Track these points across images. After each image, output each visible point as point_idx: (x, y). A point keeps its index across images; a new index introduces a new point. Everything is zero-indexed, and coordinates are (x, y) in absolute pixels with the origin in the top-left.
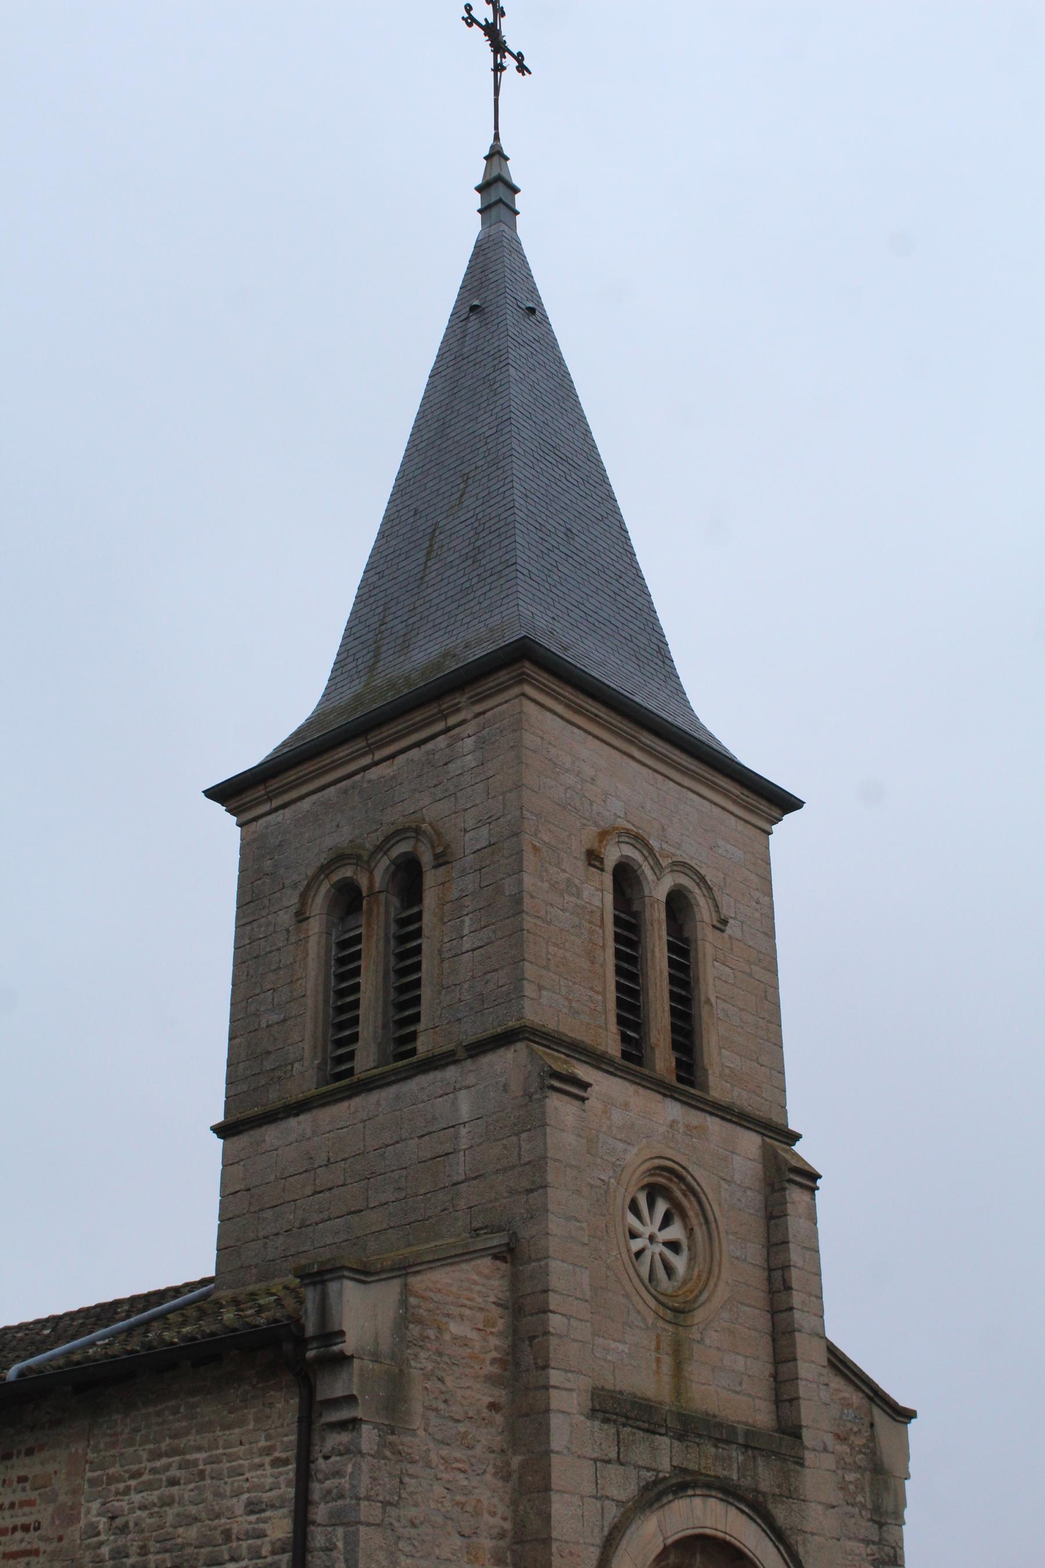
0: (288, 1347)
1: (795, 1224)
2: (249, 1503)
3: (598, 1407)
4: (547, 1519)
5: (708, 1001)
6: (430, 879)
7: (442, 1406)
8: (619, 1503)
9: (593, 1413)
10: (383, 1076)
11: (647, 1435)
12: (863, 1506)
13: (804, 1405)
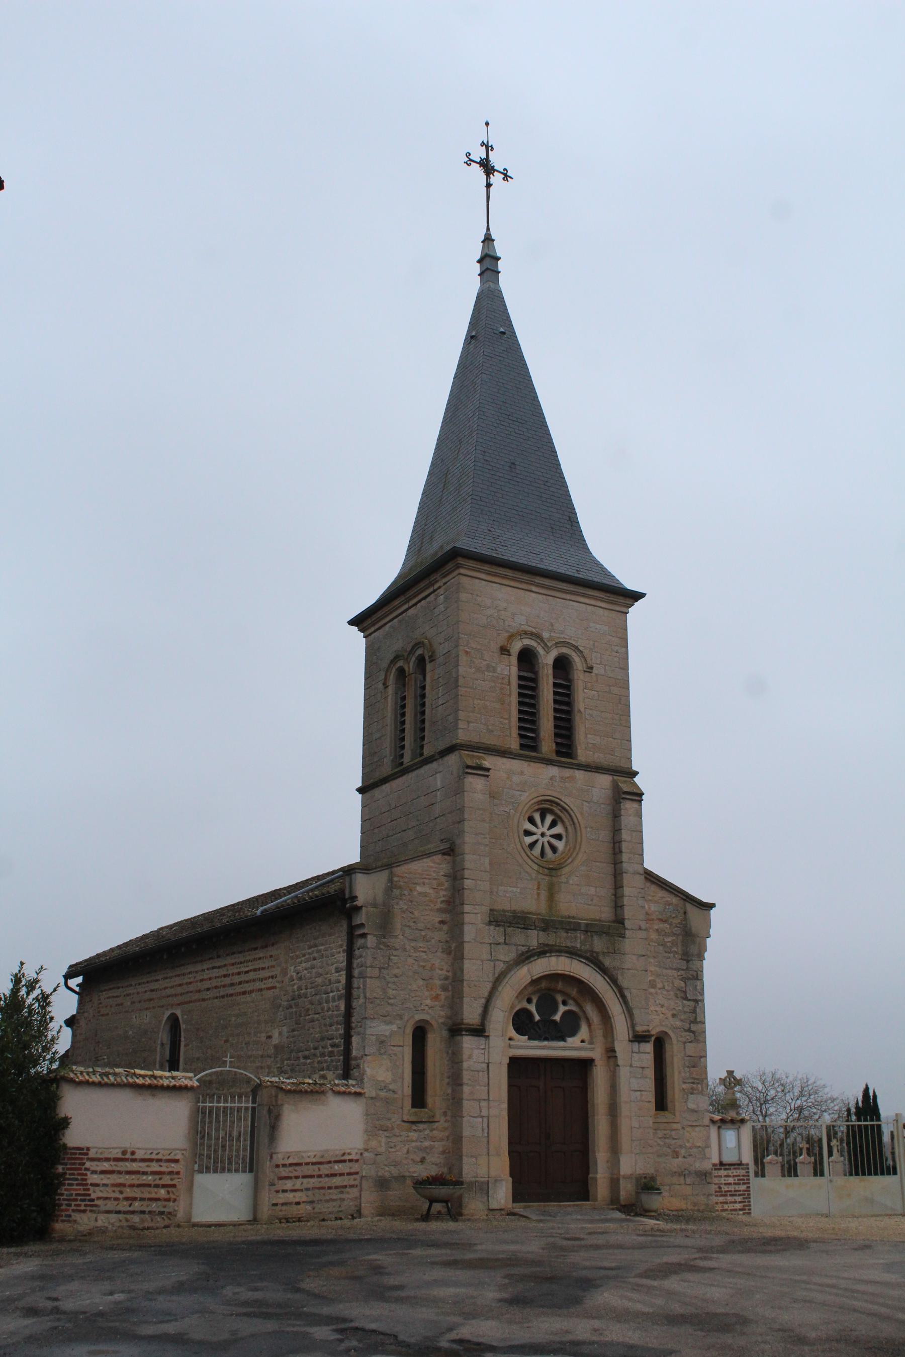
0: (339, 903)
1: (626, 820)
2: (336, 968)
4: (462, 971)
5: (579, 711)
6: (429, 667)
7: (412, 924)
9: (490, 923)
10: (396, 773)
12: (676, 953)
13: (626, 909)
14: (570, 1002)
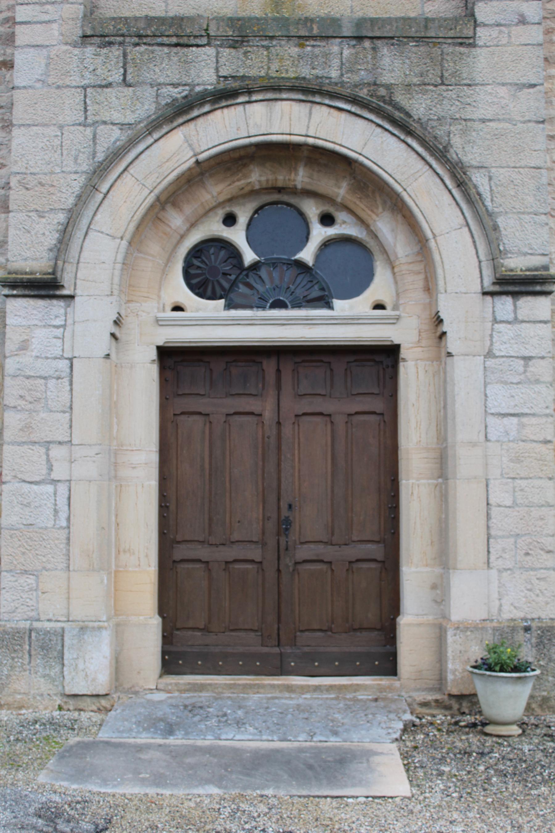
3: (89, 33)
8: (122, 126)
11: (175, 50)
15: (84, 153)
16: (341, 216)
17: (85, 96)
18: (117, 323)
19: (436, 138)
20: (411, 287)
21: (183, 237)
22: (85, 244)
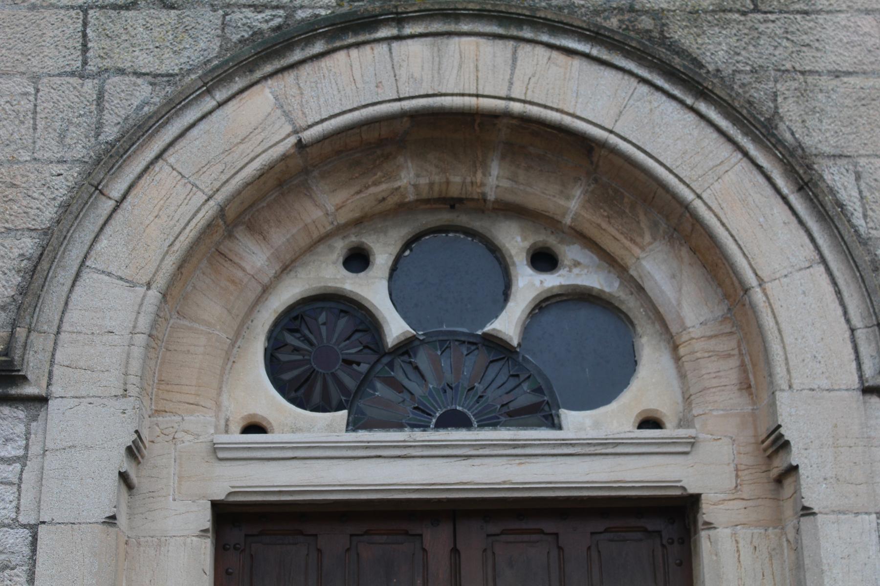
14: (570, 252)
15: (79, 125)
16: (570, 252)
17: (85, 24)
18: (133, 452)
19: (750, 103)
20: (715, 382)
21: (266, 290)
22: (74, 296)
